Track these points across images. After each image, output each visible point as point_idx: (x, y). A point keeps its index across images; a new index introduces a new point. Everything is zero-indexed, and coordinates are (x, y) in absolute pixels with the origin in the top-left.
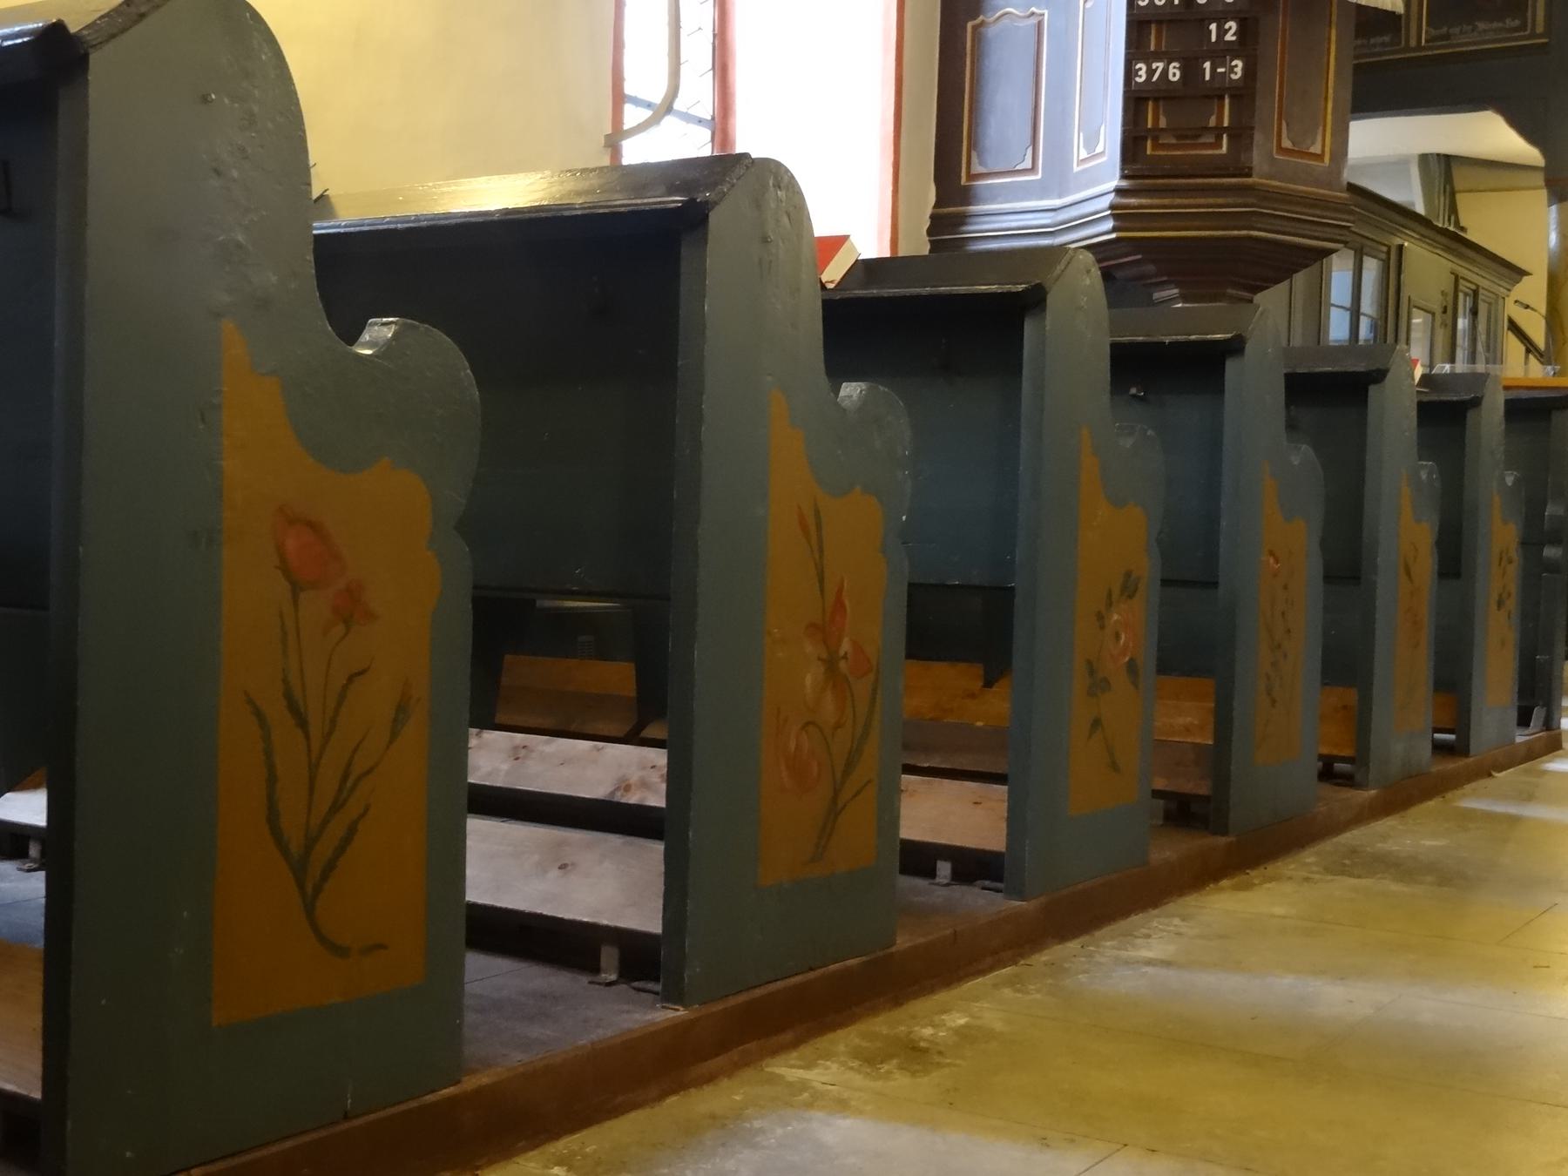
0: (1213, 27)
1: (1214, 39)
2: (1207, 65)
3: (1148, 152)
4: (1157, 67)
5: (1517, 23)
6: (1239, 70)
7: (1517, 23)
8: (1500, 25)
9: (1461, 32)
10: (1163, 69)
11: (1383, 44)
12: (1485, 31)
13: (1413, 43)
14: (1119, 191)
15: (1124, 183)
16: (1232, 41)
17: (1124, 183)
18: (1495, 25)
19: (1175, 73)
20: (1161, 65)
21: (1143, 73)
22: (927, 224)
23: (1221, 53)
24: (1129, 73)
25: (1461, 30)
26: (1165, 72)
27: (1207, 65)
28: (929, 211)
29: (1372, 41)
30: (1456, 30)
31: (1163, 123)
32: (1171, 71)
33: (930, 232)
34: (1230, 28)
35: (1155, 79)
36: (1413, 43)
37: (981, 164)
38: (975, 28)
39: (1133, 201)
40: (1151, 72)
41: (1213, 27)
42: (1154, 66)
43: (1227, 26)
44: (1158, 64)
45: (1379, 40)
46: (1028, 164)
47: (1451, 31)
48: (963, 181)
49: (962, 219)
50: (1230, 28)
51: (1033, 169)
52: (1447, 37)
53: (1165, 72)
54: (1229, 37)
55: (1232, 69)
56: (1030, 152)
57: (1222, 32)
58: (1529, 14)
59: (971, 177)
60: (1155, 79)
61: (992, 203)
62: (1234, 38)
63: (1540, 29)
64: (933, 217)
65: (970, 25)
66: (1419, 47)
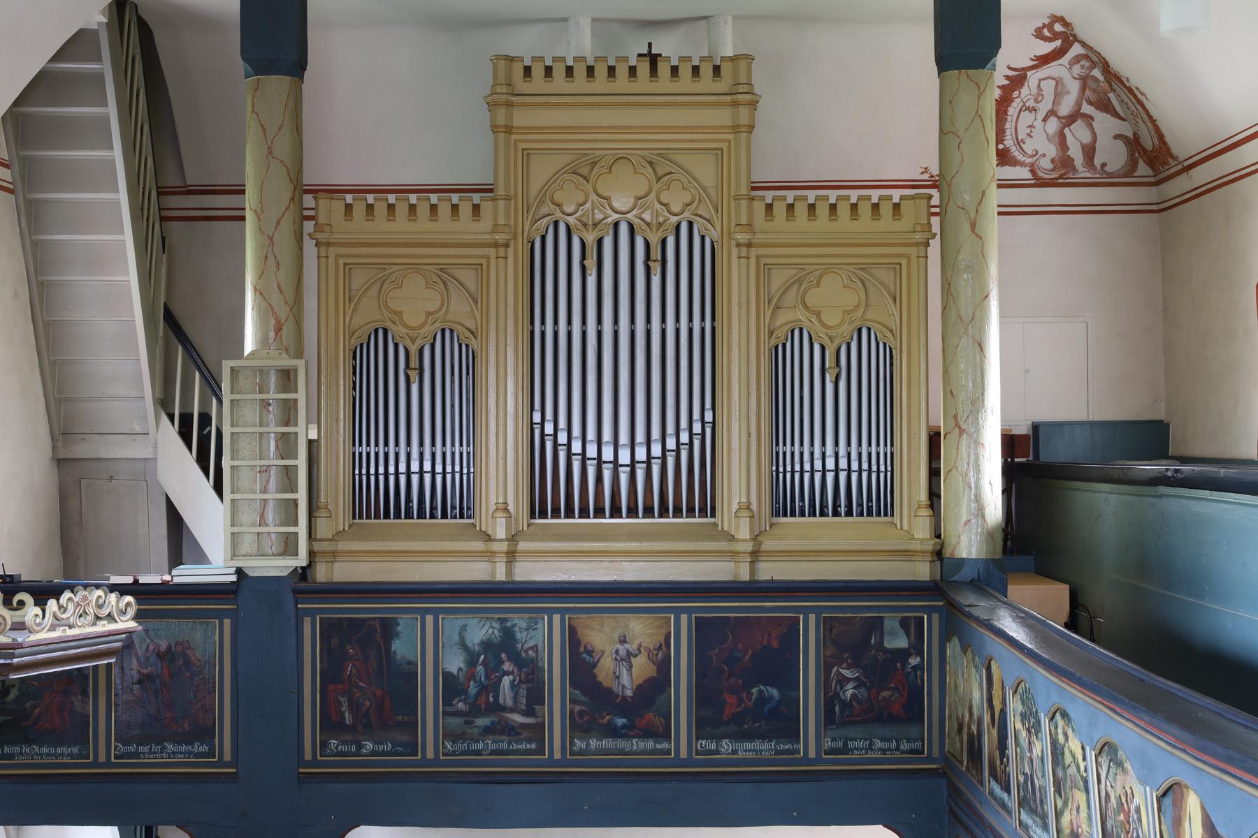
5: (205, 748)
7: (205, 748)
8: (190, 748)
9: (151, 752)
11: (71, 755)
12: (174, 753)
13: (102, 758)
18: (184, 748)
25: (151, 749)
29: (59, 751)
30: (146, 749)
45: (66, 750)
52: (135, 755)
58: (217, 740)
63: (227, 757)
66: (108, 764)
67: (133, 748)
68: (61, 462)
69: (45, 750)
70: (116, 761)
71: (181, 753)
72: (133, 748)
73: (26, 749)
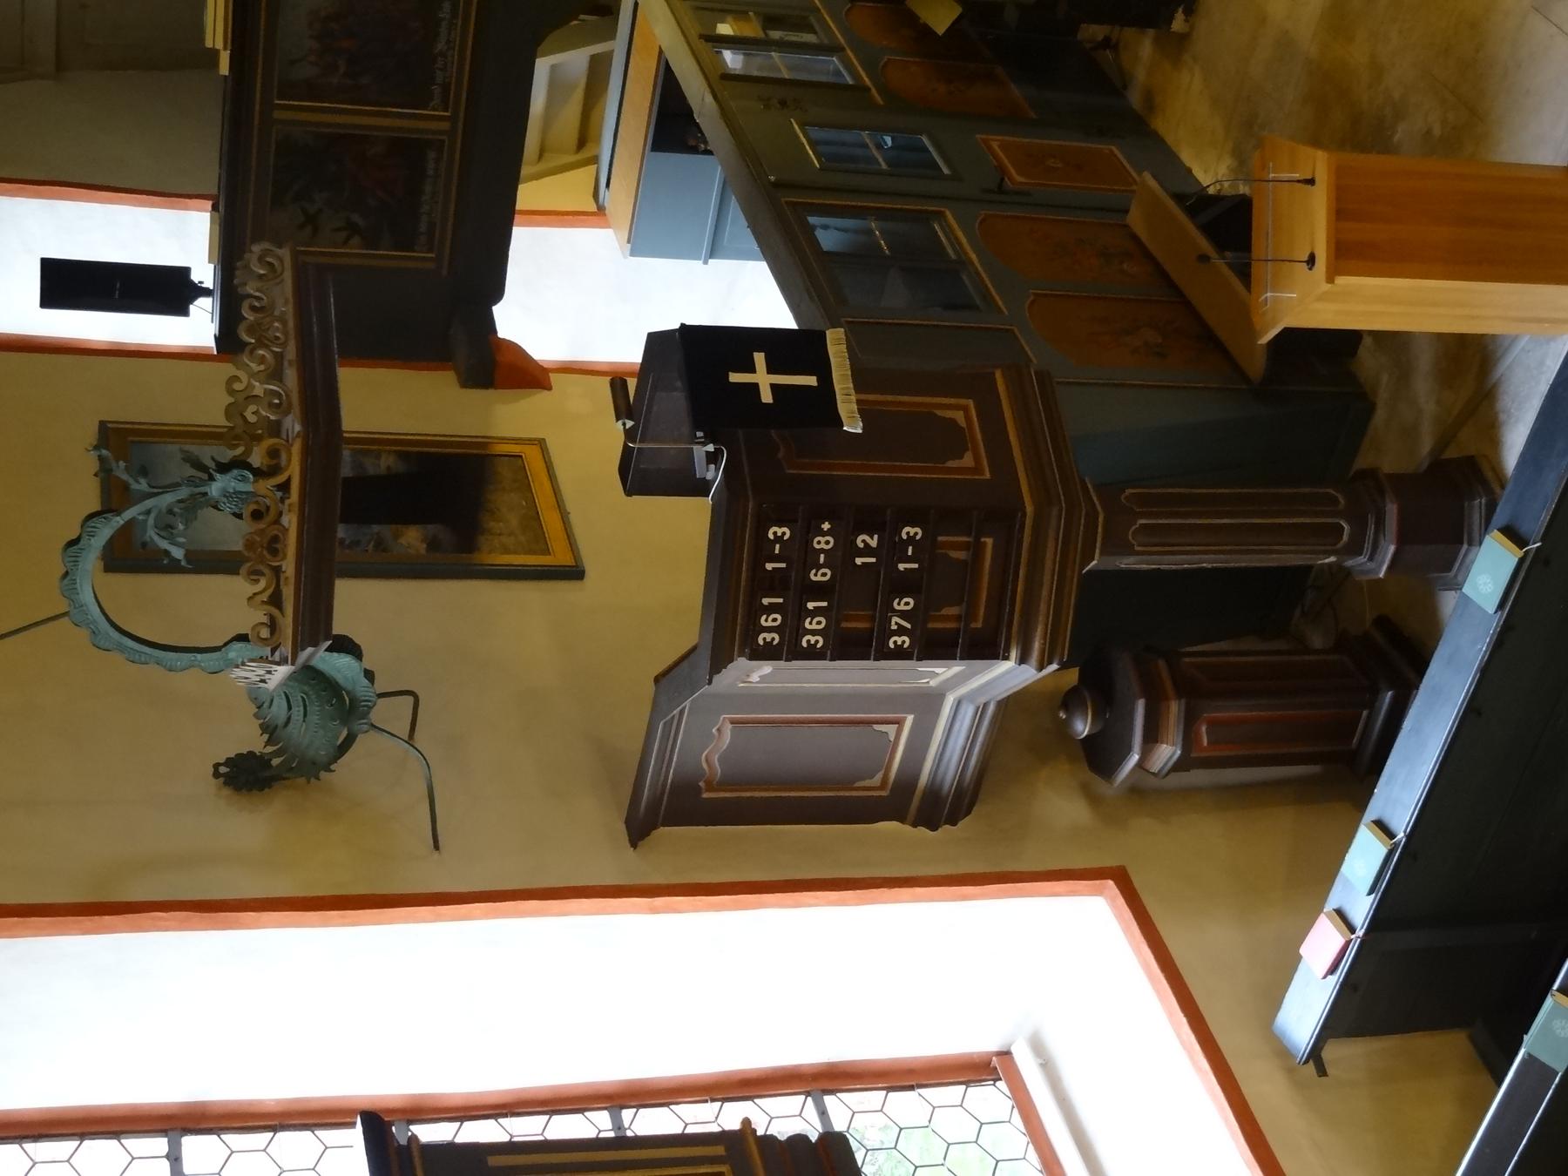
0: (859, 561)
1: (873, 560)
2: (901, 567)
3: (979, 625)
4: (896, 623)
6: (912, 531)
8: (444, 24)
10: (898, 616)
12: (448, 42)
13: (445, 126)
14: (1023, 660)
15: (1014, 654)
16: (878, 541)
17: (1014, 654)
18: (443, 29)
19: (906, 604)
20: (895, 619)
21: (899, 640)
22: (922, 830)
23: (892, 549)
24: (900, 654)
26: (903, 615)
27: (901, 567)
28: (907, 828)
29: (430, 172)
31: (953, 611)
32: (902, 607)
33: (934, 828)
34: (863, 541)
35: (909, 626)
36: (445, 126)
37: (872, 777)
38: (710, 788)
39: (1037, 645)
40: (901, 631)
41: (859, 561)
42: (894, 627)
43: (861, 545)
44: (893, 623)
45: (431, 165)
46: (891, 729)
47: (439, 80)
48: (884, 793)
49: (933, 793)
50: (863, 541)
51: (899, 723)
52: (446, 88)
53: (903, 615)
54: (874, 543)
55: (911, 539)
56: (876, 727)
57: (867, 550)
59: (883, 786)
60: (909, 626)
61: (924, 759)
62: (876, 537)
64: (915, 825)
65: (705, 795)
66: (453, 119)
67: (436, 89)
68: (61, 66)
69: (428, 188)
70: (450, 110)
71: (449, 34)
72: (436, 89)
73: (426, 208)
